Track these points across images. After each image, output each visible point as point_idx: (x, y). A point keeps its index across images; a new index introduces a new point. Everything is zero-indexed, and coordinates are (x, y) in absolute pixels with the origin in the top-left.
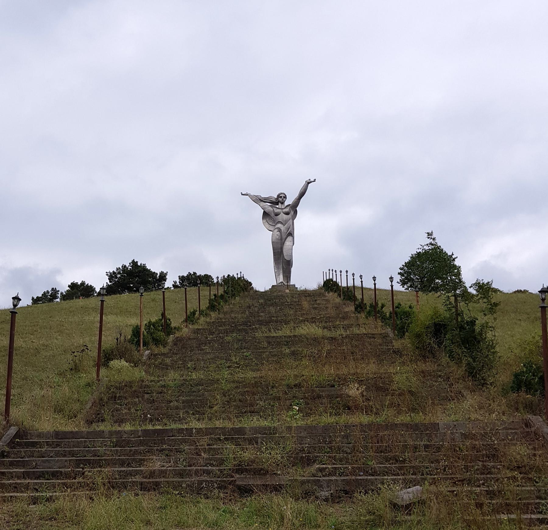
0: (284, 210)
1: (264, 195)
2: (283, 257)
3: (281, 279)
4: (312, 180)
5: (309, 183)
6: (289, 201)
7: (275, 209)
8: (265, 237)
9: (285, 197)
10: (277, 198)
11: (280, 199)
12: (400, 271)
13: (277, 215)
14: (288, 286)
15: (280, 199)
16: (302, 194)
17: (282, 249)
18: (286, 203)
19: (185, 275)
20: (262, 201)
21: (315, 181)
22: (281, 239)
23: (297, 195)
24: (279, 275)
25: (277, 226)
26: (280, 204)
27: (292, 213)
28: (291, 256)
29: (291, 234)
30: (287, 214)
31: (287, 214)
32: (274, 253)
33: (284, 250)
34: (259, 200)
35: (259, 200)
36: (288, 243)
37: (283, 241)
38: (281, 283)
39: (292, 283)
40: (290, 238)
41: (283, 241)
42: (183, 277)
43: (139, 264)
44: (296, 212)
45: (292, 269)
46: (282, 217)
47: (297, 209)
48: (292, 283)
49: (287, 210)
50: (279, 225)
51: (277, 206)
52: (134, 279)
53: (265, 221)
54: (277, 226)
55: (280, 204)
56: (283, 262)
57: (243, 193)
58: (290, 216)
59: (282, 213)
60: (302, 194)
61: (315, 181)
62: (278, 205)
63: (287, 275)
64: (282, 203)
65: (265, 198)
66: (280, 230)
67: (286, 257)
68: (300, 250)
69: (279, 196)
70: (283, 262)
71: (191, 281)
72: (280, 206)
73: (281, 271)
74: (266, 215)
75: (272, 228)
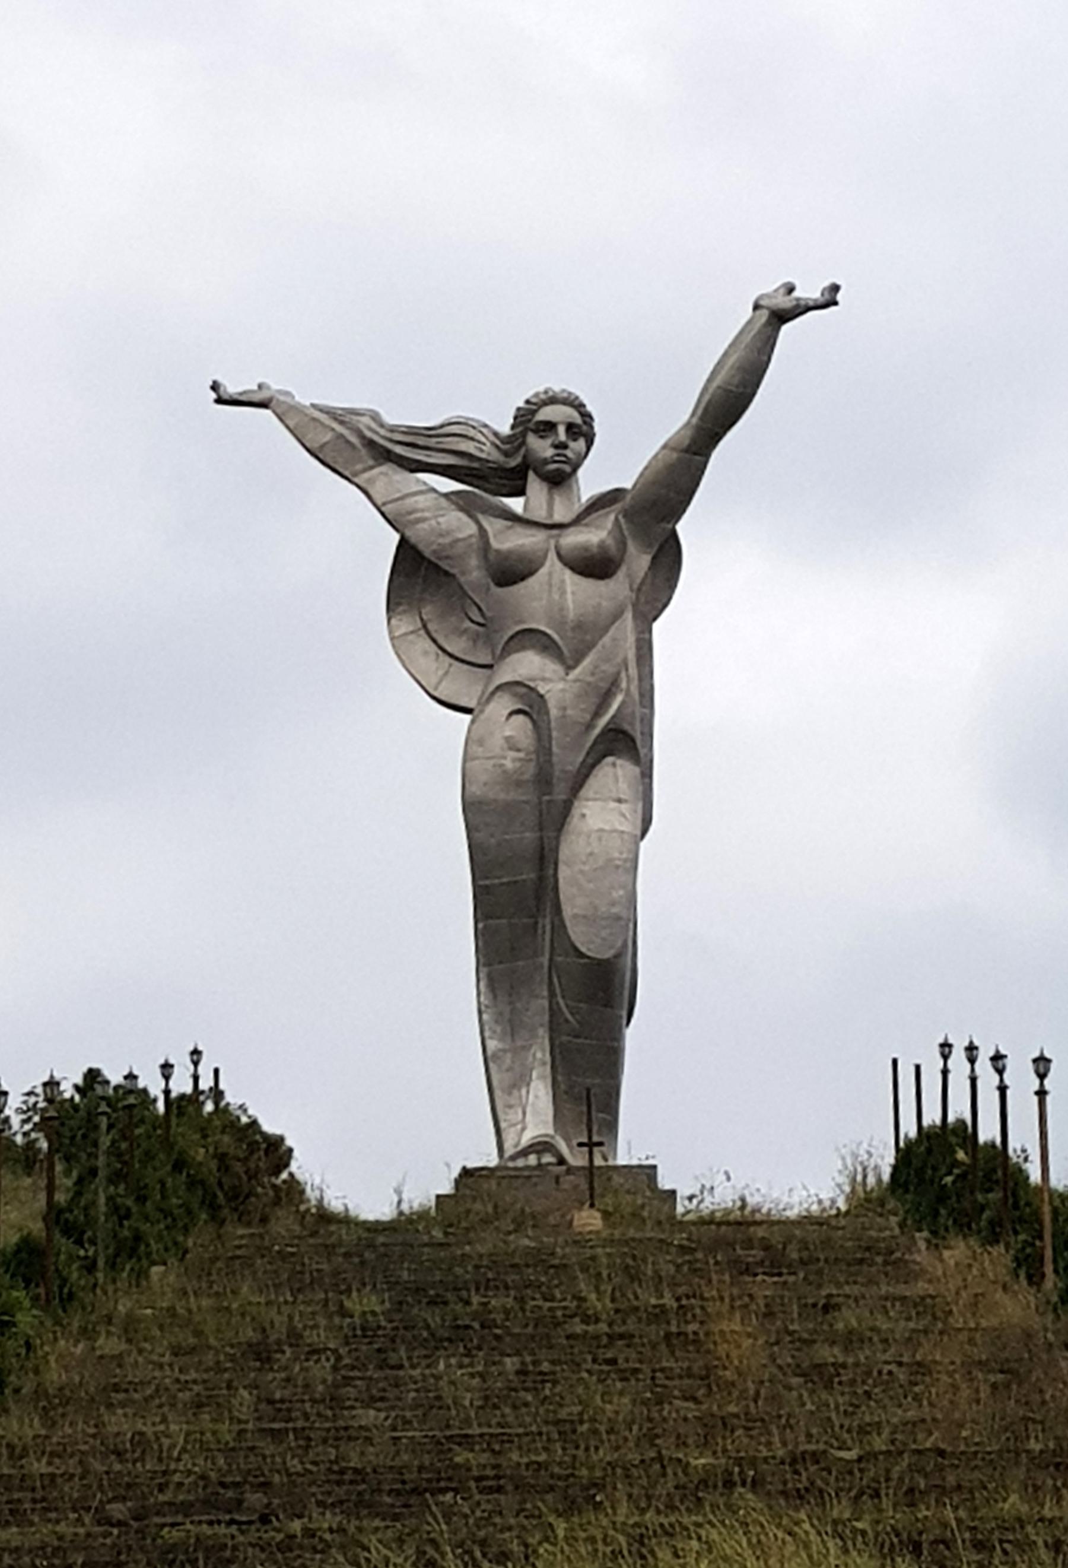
2: (559, 927)
4: (809, 291)
5: (781, 317)
6: (613, 465)
7: (492, 525)
9: (583, 430)
11: (542, 444)
13: (510, 572)
14: (599, 1182)
15: (542, 447)
16: (724, 408)
17: (545, 858)
18: (593, 479)
21: (830, 299)
23: (676, 414)
24: (521, 1080)
25: (506, 673)
26: (535, 485)
29: (625, 740)
30: (595, 566)
31: (595, 566)
32: (480, 894)
33: (563, 872)
36: (598, 814)
37: (560, 794)
38: (540, 1147)
44: (668, 559)
46: (555, 593)
47: (687, 529)
51: (516, 504)
53: (406, 624)
54: (506, 673)
55: (535, 485)
56: (556, 973)
57: (232, 389)
58: (616, 589)
59: (552, 556)
60: (724, 408)
61: (830, 299)
62: (520, 492)
63: (589, 1084)
64: (560, 479)
65: (418, 437)
67: (579, 935)
68: (695, 878)
69: (528, 420)
70: (556, 973)
73: (540, 1053)
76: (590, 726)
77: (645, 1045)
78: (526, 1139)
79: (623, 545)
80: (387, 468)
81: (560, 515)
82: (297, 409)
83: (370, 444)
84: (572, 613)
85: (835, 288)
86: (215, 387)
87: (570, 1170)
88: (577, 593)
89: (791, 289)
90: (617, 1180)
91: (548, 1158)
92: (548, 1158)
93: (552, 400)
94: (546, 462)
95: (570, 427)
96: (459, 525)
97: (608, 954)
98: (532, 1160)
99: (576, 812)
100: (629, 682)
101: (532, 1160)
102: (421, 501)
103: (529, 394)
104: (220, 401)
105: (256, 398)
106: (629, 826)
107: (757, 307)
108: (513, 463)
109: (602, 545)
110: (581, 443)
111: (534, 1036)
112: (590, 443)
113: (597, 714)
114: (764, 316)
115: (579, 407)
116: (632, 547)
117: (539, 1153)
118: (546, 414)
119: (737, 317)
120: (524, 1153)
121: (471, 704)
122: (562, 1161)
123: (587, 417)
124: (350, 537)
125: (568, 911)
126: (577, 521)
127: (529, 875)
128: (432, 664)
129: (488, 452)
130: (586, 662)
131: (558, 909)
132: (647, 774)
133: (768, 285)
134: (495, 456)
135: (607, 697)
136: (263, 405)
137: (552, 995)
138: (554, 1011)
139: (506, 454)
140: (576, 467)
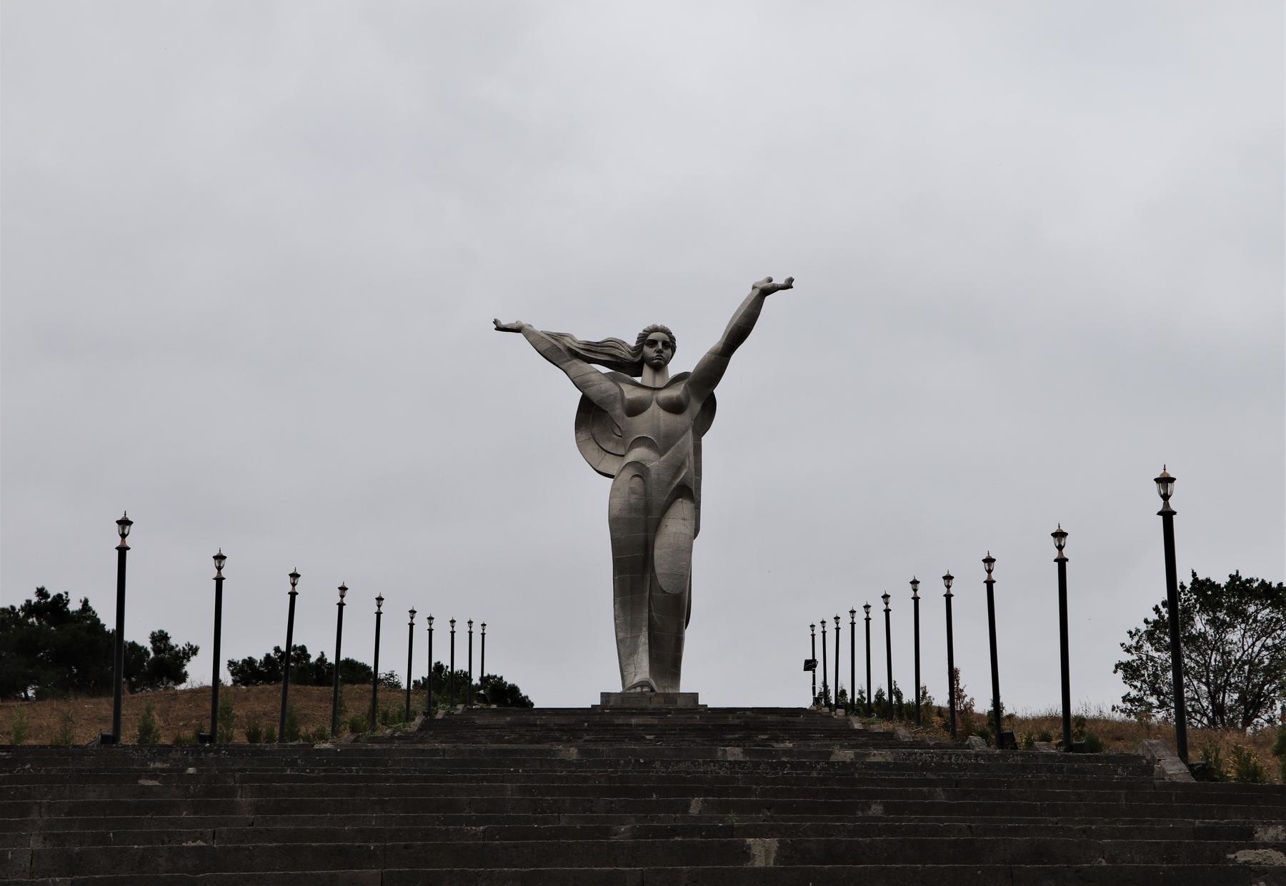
0: (664, 394)
1: (586, 332)
2: (654, 579)
3: (642, 670)
4: (779, 280)
6: (684, 361)
9: (670, 344)
10: (638, 349)
12: (1126, 658)
13: (635, 409)
15: (650, 352)
16: (738, 334)
17: (647, 548)
18: (674, 368)
19: (259, 657)
21: (788, 285)
22: (647, 509)
23: (714, 337)
24: (634, 652)
27: (696, 406)
29: (688, 491)
30: (675, 407)
32: (617, 562)
33: (657, 553)
34: (558, 351)
35: (558, 351)
36: (674, 526)
37: (655, 515)
38: (642, 684)
39: (685, 686)
40: (682, 507)
42: (250, 662)
43: (74, 606)
44: (709, 407)
45: (689, 634)
46: (654, 419)
48: (685, 686)
49: (676, 392)
50: (638, 453)
51: (638, 379)
53: (584, 436)
55: (647, 371)
56: (652, 600)
57: (504, 323)
58: (685, 419)
59: (654, 403)
60: (738, 334)
61: (788, 285)
62: (640, 374)
63: (667, 657)
64: (659, 367)
65: (590, 347)
66: (640, 469)
67: (663, 582)
68: (719, 560)
69: (644, 339)
70: (652, 600)
72: (647, 377)
73: (644, 639)
74: (592, 416)
75: (613, 466)
76: (670, 483)
77: (693, 638)
78: (637, 680)
79: (689, 401)
80: (575, 361)
81: (659, 383)
82: (534, 333)
83: (570, 350)
84: (663, 428)
85: (791, 280)
86: (495, 322)
87: (657, 695)
89: (770, 280)
90: (679, 701)
91: (645, 689)
92: (645, 689)
93: (656, 330)
94: (653, 359)
95: (664, 343)
96: (608, 385)
97: (677, 592)
98: (639, 689)
99: (663, 524)
101: (639, 689)
102: (593, 377)
103: (645, 327)
104: (498, 329)
105: (515, 327)
106: (690, 531)
107: (754, 288)
108: (637, 360)
109: (678, 398)
110: (669, 351)
111: (641, 630)
112: (674, 350)
113: (674, 477)
114: (757, 292)
115: (668, 333)
116: (692, 400)
117: (642, 686)
118: (652, 336)
119: (741, 296)
120: (635, 687)
121: (614, 473)
122: (652, 690)
123: (673, 339)
124: (561, 395)
125: (658, 570)
126: (666, 387)
129: (626, 355)
130: (670, 452)
131: (653, 570)
132: (697, 508)
133: (760, 278)
134: (629, 356)
135: (679, 469)
136: (518, 330)
137: (650, 611)
138: (650, 619)
139: (634, 356)
140: (667, 362)
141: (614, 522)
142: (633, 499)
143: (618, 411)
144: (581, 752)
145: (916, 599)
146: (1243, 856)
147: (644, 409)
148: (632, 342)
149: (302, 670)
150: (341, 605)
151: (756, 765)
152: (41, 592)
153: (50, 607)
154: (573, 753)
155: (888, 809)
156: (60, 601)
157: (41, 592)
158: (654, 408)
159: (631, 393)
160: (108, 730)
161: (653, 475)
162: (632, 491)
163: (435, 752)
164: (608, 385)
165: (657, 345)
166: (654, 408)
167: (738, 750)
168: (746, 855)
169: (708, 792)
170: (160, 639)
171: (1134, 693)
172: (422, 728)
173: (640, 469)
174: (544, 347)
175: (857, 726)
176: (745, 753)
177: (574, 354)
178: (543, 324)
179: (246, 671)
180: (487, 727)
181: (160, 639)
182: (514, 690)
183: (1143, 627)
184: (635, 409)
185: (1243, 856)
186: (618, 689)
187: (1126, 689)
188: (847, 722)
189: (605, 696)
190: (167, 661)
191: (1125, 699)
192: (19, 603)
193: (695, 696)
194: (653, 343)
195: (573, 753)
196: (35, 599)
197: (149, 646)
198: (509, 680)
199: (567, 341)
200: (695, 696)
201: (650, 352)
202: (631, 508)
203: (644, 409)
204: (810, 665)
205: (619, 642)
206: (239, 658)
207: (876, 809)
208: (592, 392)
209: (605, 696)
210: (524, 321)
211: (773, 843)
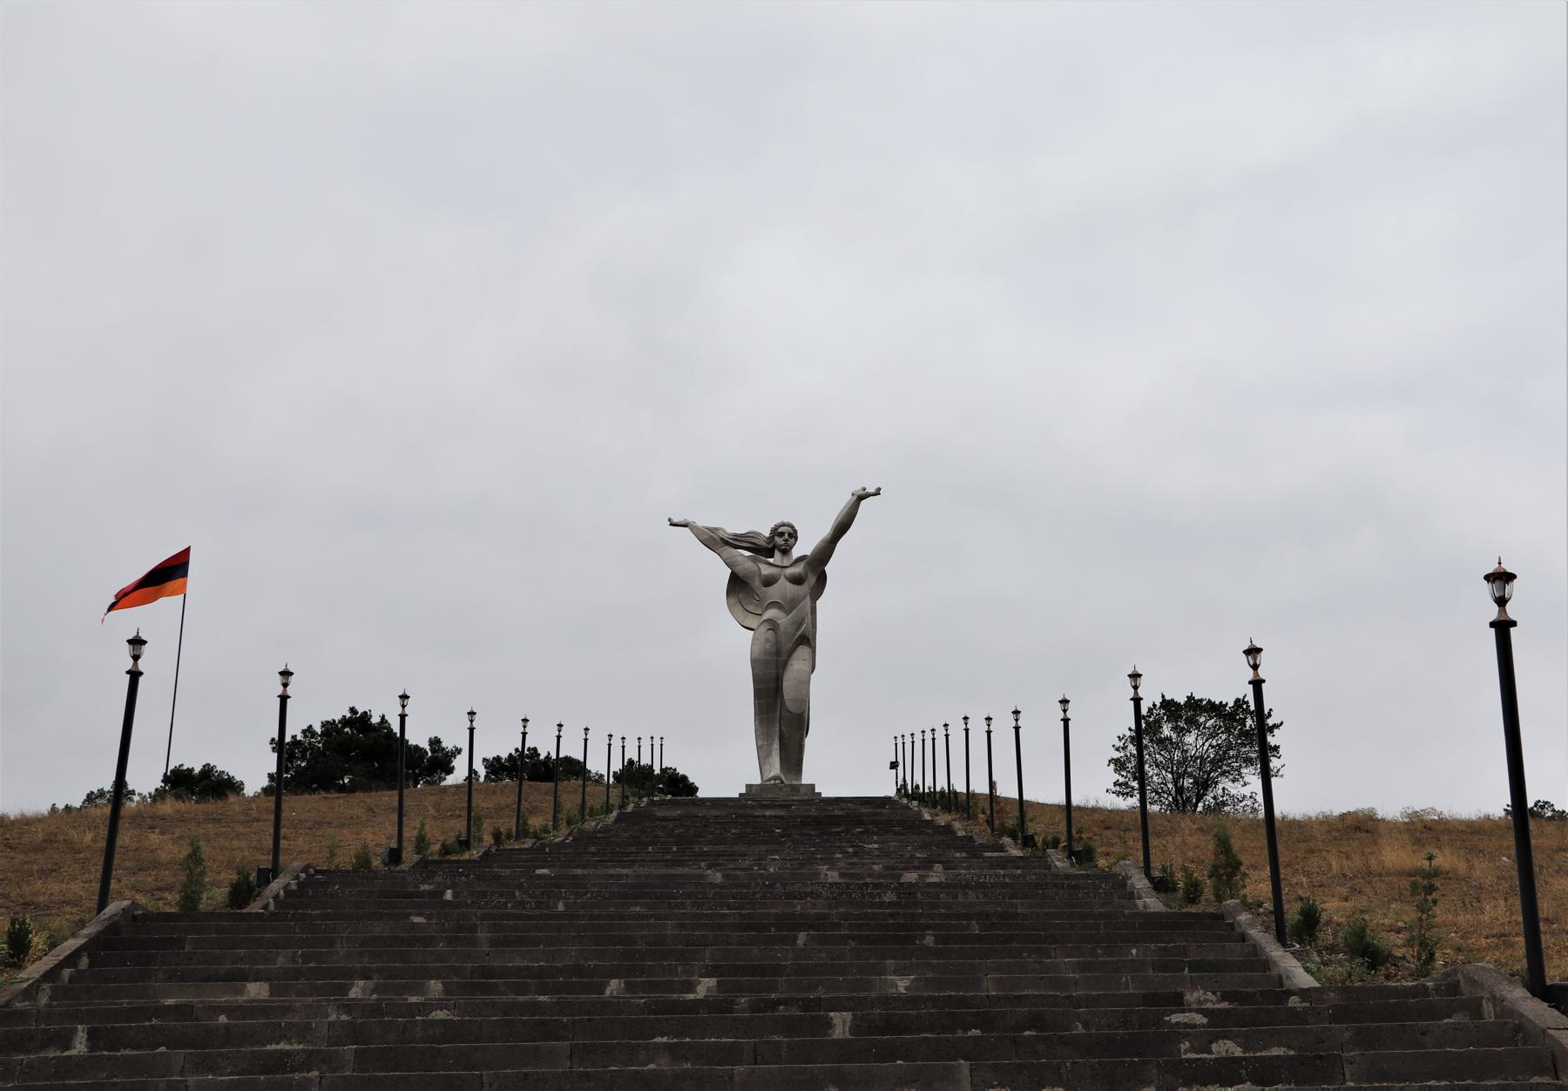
0: (789, 571)
2: (783, 703)
3: (775, 768)
4: (872, 490)
5: (861, 498)
6: (804, 547)
8: (733, 645)
9: (793, 535)
10: (771, 538)
12: (1117, 755)
13: (769, 582)
14: (796, 788)
15: (779, 540)
16: (842, 528)
18: (797, 552)
19: (504, 756)
20: (726, 543)
21: (877, 493)
22: (778, 653)
23: (826, 530)
24: (769, 755)
27: (812, 580)
28: (805, 702)
29: (807, 640)
30: (797, 580)
34: (715, 541)
35: (715, 541)
36: (797, 664)
37: (783, 658)
38: (775, 778)
39: (806, 779)
40: (803, 651)
41: (783, 658)
42: (498, 759)
43: (375, 720)
45: (808, 741)
46: (783, 588)
48: (806, 779)
50: (771, 613)
52: (356, 755)
53: (733, 600)
55: (777, 554)
56: (781, 717)
57: (675, 520)
58: (804, 589)
60: (842, 528)
61: (877, 493)
63: (792, 757)
64: (786, 552)
65: (737, 537)
66: (773, 625)
67: (789, 705)
68: (828, 688)
69: (776, 532)
70: (781, 717)
71: (524, 768)
72: (777, 558)
74: (738, 585)
84: (789, 595)
88: (791, 589)
100: (808, 620)
106: (809, 669)
119: (845, 500)
124: (718, 572)
125: (786, 696)
127: (773, 685)
128: (741, 613)
129: (762, 543)
132: (814, 652)
135: (800, 625)
141: (754, 662)
142: (768, 646)
143: (757, 583)
144: (725, 876)
145: (967, 730)
146: (1176, 1018)
147: (777, 580)
148: (767, 534)
149: (534, 765)
150: (559, 737)
151: (848, 885)
152: (353, 710)
153: (359, 721)
154: (718, 877)
155: (938, 939)
156: (366, 716)
157: (353, 710)
158: (783, 582)
159: (766, 570)
160: (394, 845)
161: (782, 629)
162: (767, 640)
163: (619, 877)
164: (750, 564)
165: (783, 537)
166: (783, 582)
167: (835, 874)
168: (829, 1025)
169: (811, 927)
170: (435, 742)
171: (1122, 780)
172: (618, 820)
173: (773, 625)
174: (704, 537)
175: (927, 817)
176: (842, 875)
177: (726, 543)
178: (703, 521)
179: (496, 767)
180: (664, 819)
181: (435, 742)
182: (684, 778)
183: (1128, 734)
184: (769, 582)
185: (1176, 1018)
186: (758, 781)
187: (1116, 777)
188: (919, 814)
189: (749, 787)
190: (440, 760)
191: (1115, 784)
192: (338, 718)
193: (812, 786)
194: (782, 534)
195: (718, 877)
196: (348, 715)
197: (428, 748)
198: (681, 771)
199: (721, 534)
200: (812, 786)
201: (779, 540)
202: (766, 652)
203: (777, 580)
204: (894, 765)
205: (758, 748)
206: (490, 756)
207: (929, 940)
208: (738, 569)
209: (749, 787)
210: (690, 520)
211: (848, 1016)
